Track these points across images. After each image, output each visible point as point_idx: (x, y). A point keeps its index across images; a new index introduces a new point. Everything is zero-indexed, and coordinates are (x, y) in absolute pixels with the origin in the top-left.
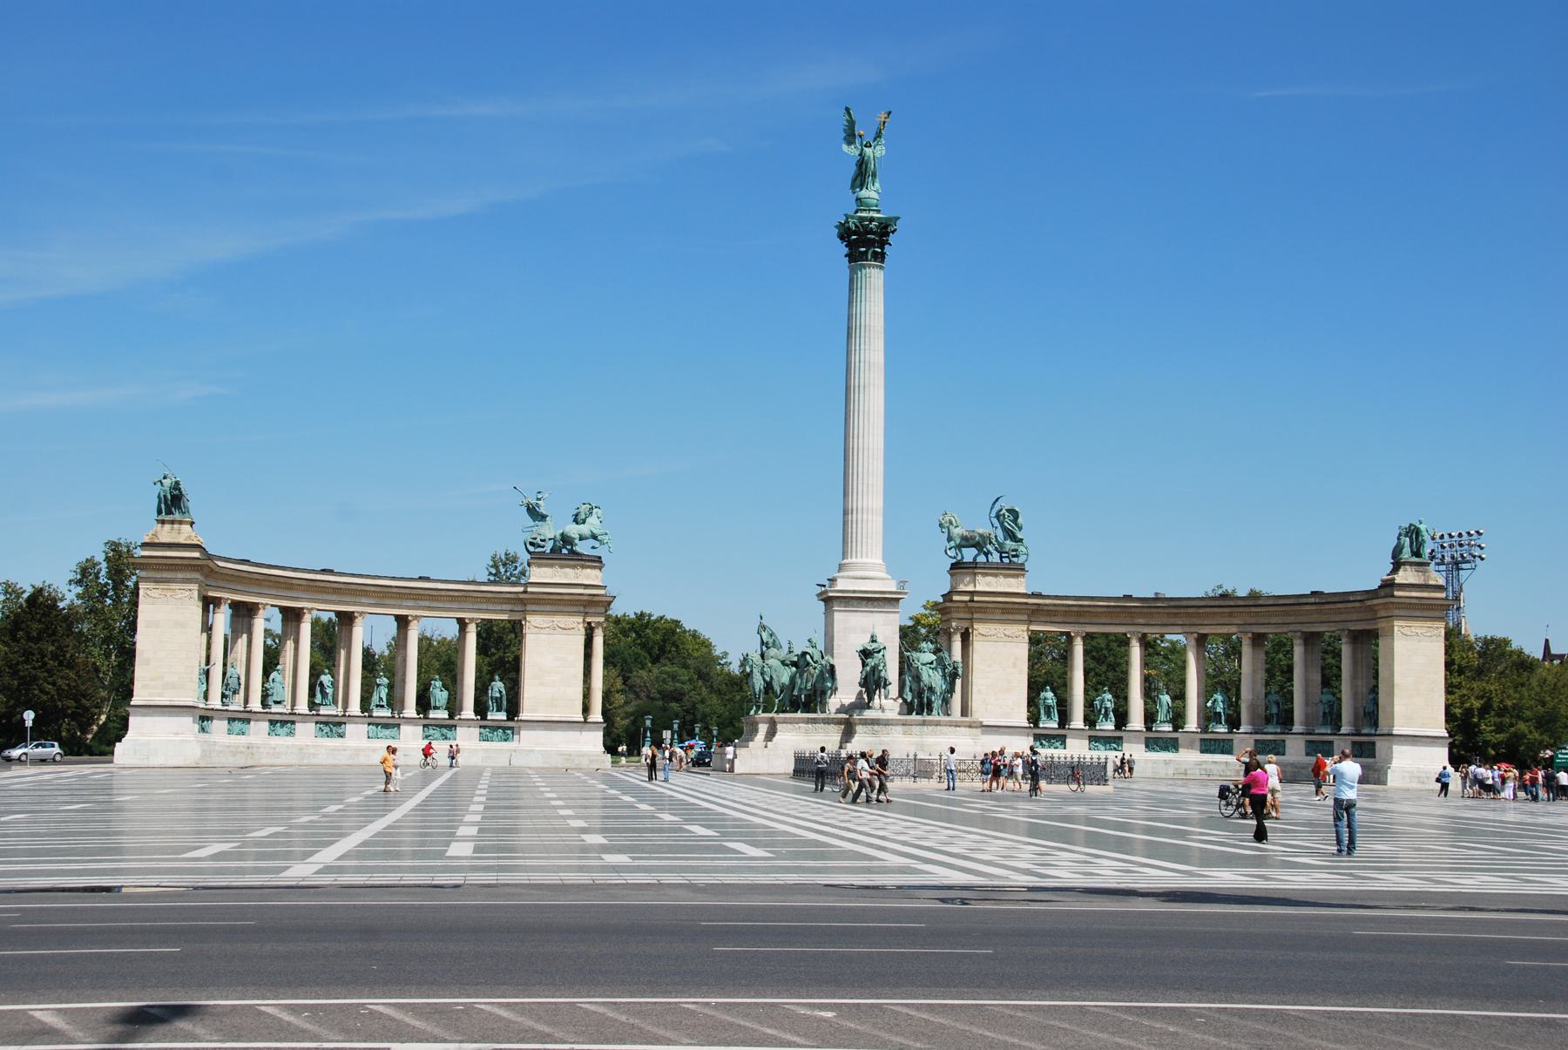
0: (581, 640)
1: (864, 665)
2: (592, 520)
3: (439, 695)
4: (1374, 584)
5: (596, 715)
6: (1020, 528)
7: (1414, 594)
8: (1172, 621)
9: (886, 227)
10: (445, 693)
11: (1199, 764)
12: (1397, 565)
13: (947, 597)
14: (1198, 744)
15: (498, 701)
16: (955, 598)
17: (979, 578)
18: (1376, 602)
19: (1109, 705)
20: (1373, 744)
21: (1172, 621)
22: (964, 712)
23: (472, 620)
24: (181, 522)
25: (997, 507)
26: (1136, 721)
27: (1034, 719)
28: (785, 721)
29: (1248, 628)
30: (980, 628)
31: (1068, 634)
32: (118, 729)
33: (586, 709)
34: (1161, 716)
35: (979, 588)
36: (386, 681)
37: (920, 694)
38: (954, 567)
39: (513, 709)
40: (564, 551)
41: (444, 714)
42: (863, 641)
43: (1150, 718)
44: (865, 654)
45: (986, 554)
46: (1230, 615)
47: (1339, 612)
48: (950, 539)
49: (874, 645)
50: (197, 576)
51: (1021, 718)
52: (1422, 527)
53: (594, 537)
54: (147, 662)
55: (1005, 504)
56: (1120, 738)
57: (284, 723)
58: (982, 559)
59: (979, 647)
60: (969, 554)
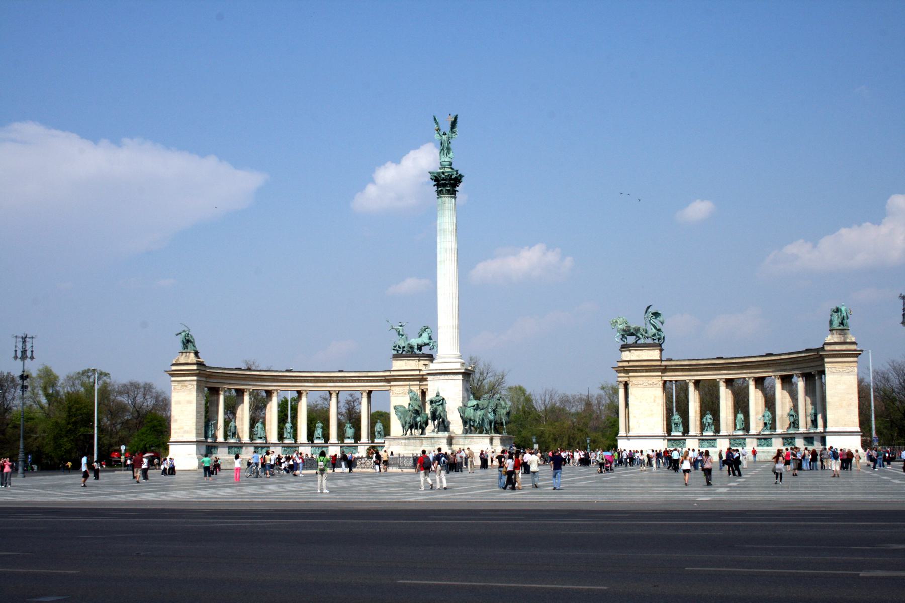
7: (837, 347)
19: (710, 421)
27: (669, 430)
30: (633, 382)
34: (738, 427)
36: (321, 424)
50: (195, 378)
52: (843, 308)
54: (176, 421)
55: (651, 310)
57: (263, 448)
59: (631, 391)
60: (631, 340)
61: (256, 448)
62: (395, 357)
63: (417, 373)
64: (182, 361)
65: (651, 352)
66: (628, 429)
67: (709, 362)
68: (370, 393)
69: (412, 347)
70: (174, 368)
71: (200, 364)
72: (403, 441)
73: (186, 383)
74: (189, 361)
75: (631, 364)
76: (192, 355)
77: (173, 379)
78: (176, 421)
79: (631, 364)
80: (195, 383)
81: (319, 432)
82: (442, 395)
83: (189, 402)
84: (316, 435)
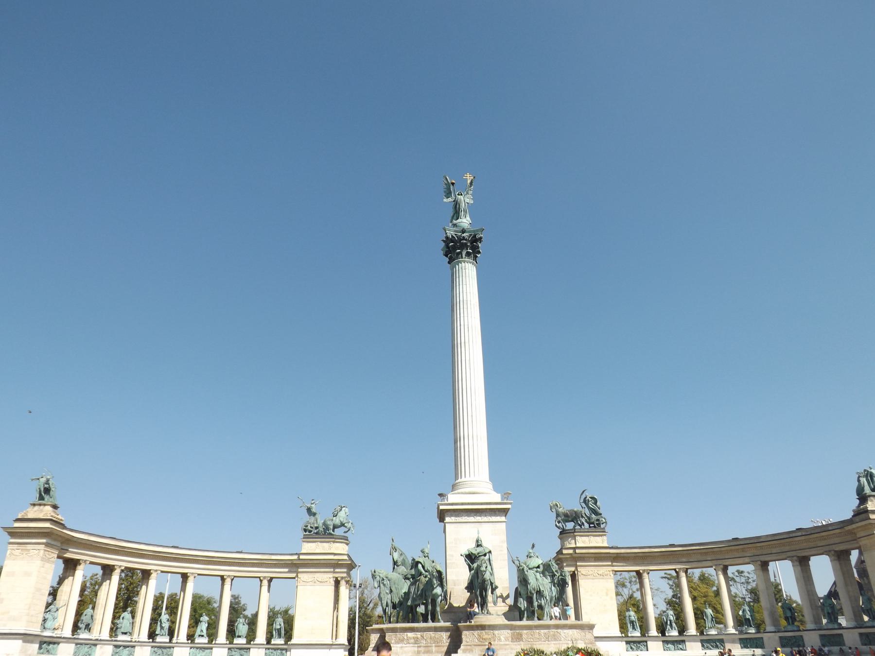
1: (470, 569)
3: (242, 628)
4: (849, 515)
5: (343, 639)
8: (704, 558)
9: (475, 236)
10: (246, 627)
12: (863, 498)
13: (560, 552)
15: (279, 631)
16: (565, 552)
17: (578, 538)
18: (854, 526)
21: (704, 558)
23: (265, 578)
24: (45, 505)
26: (692, 630)
28: (394, 630)
29: (757, 558)
31: (638, 572)
35: (578, 545)
37: (530, 600)
39: (289, 636)
40: (325, 533)
41: (243, 641)
42: (469, 546)
44: (471, 558)
45: (580, 526)
46: (743, 550)
47: (823, 538)
48: (558, 515)
49: (479, 549)
50: (44, 541)
51: (616, 631)
53: (343, 525)
55: (588, 495)
56: (684, 641)
59: (582, 583)
60: (570, 526)
61: (116, 646)
64: (30, 516)
65: (599, 539)
67: (663, 550)
68: (270, 580)
69: (327, 528)
70: (17, 525)
72: (410, 635)
74: (41, 516)
75: (577, 551)
76: (48, 509)
79: (577, 551)
81: (203, 626)
82: (487, 544)
84: (198, 632)
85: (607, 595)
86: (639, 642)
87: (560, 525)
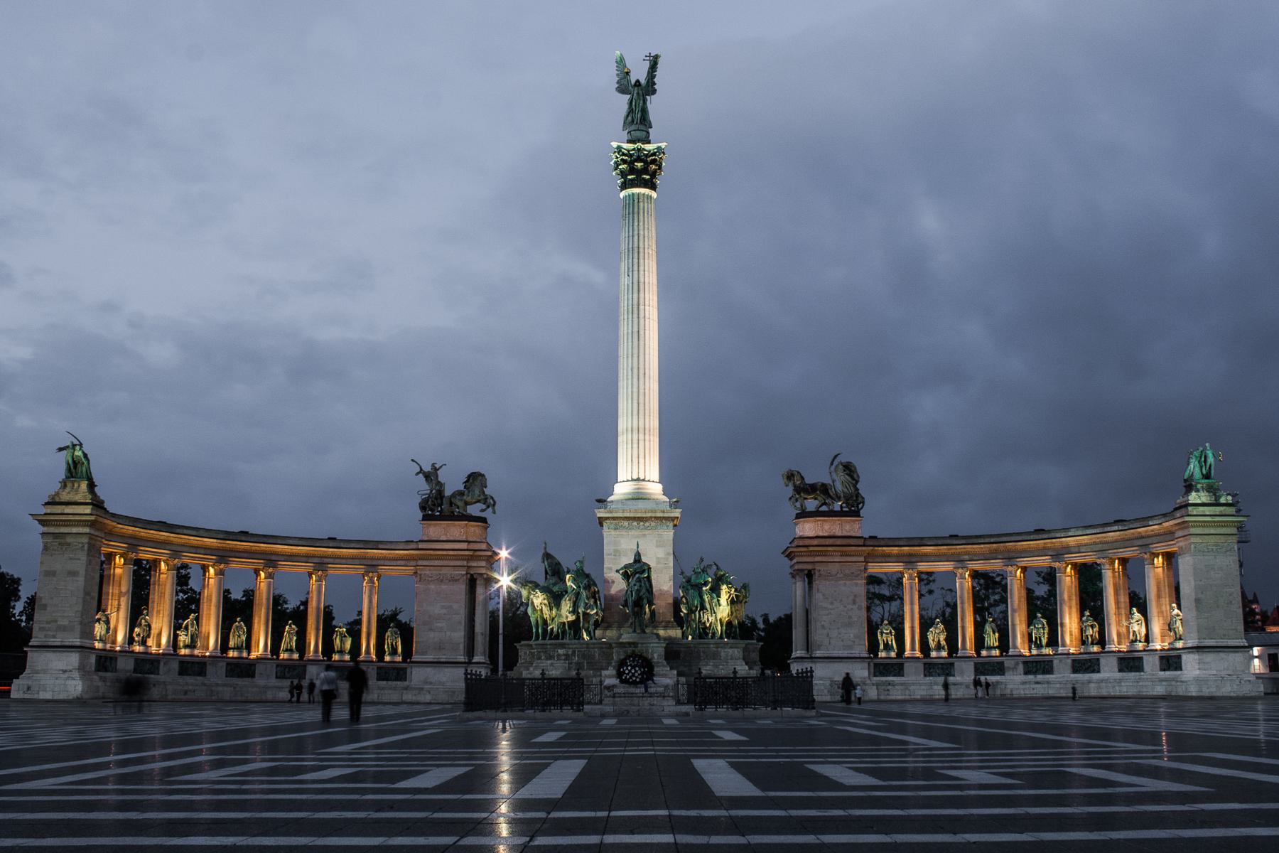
0: (462, 588)
2: (478, 483)
6: (857, 482)
11: (1025, 683)
14: (1021, 667)
20: (1179, 657)
22: (808, 647)
25: (836, 463)
32: (19, 666)
33: (470, 651)
38: (798, 516)
43: (980, 643)
50: (87, 530)
51: (862, 650)
54: (44, 607)
55: (843, 459)
58: (824, 508)
60: (811, 504)
62: (426, 518)
63: (464, 546)
64: (65, 497)
66: (808, 647)
71: (98, 504)
73: (69, 540)
74: (78, 498)
75: (816, 542)
77: (45, 529)
78: (44, 607)
79: (816, 542)
80: (85, 540)
83: (73, 574)
85: (854, 602)
86: (893, 665)
87: (798, 504)
